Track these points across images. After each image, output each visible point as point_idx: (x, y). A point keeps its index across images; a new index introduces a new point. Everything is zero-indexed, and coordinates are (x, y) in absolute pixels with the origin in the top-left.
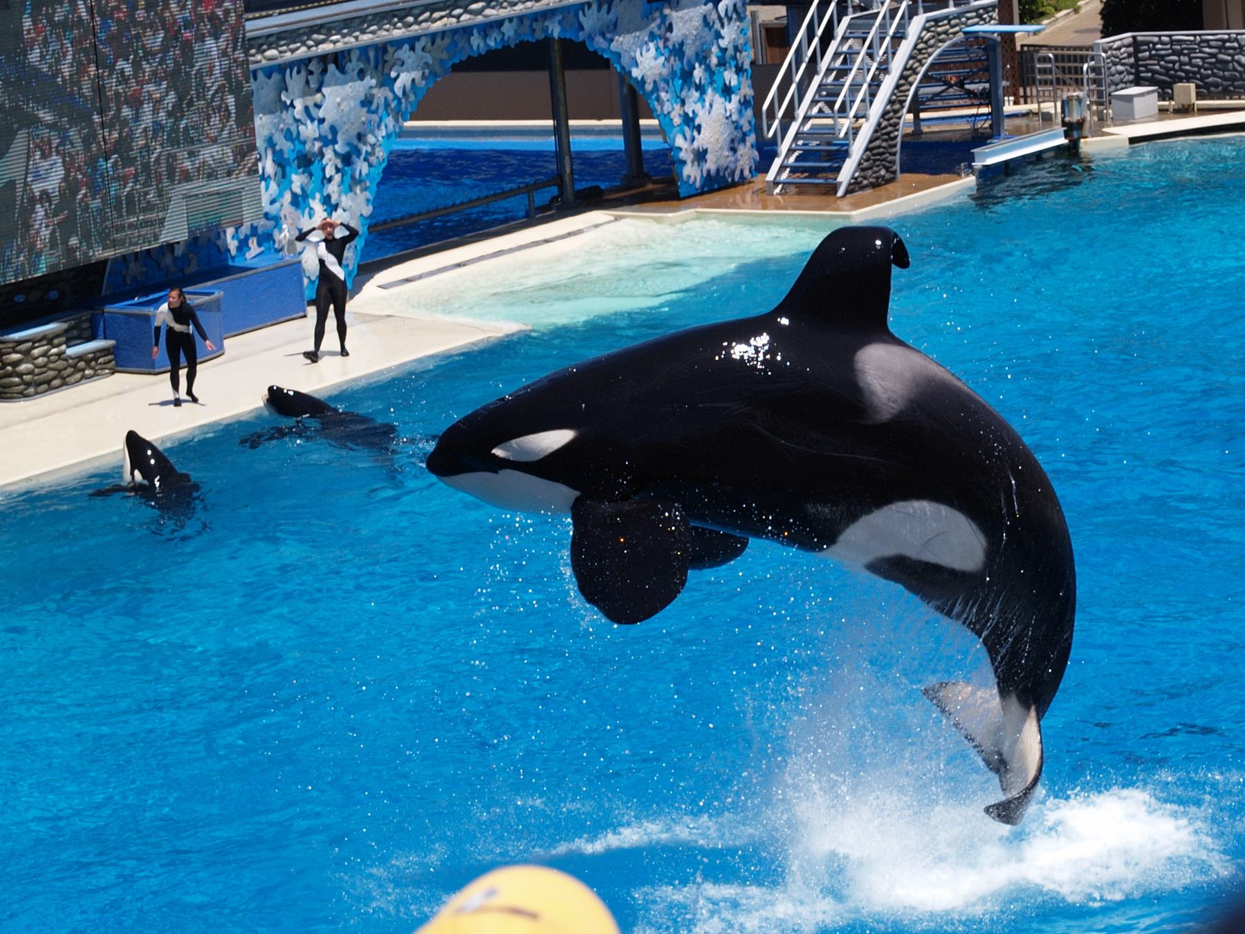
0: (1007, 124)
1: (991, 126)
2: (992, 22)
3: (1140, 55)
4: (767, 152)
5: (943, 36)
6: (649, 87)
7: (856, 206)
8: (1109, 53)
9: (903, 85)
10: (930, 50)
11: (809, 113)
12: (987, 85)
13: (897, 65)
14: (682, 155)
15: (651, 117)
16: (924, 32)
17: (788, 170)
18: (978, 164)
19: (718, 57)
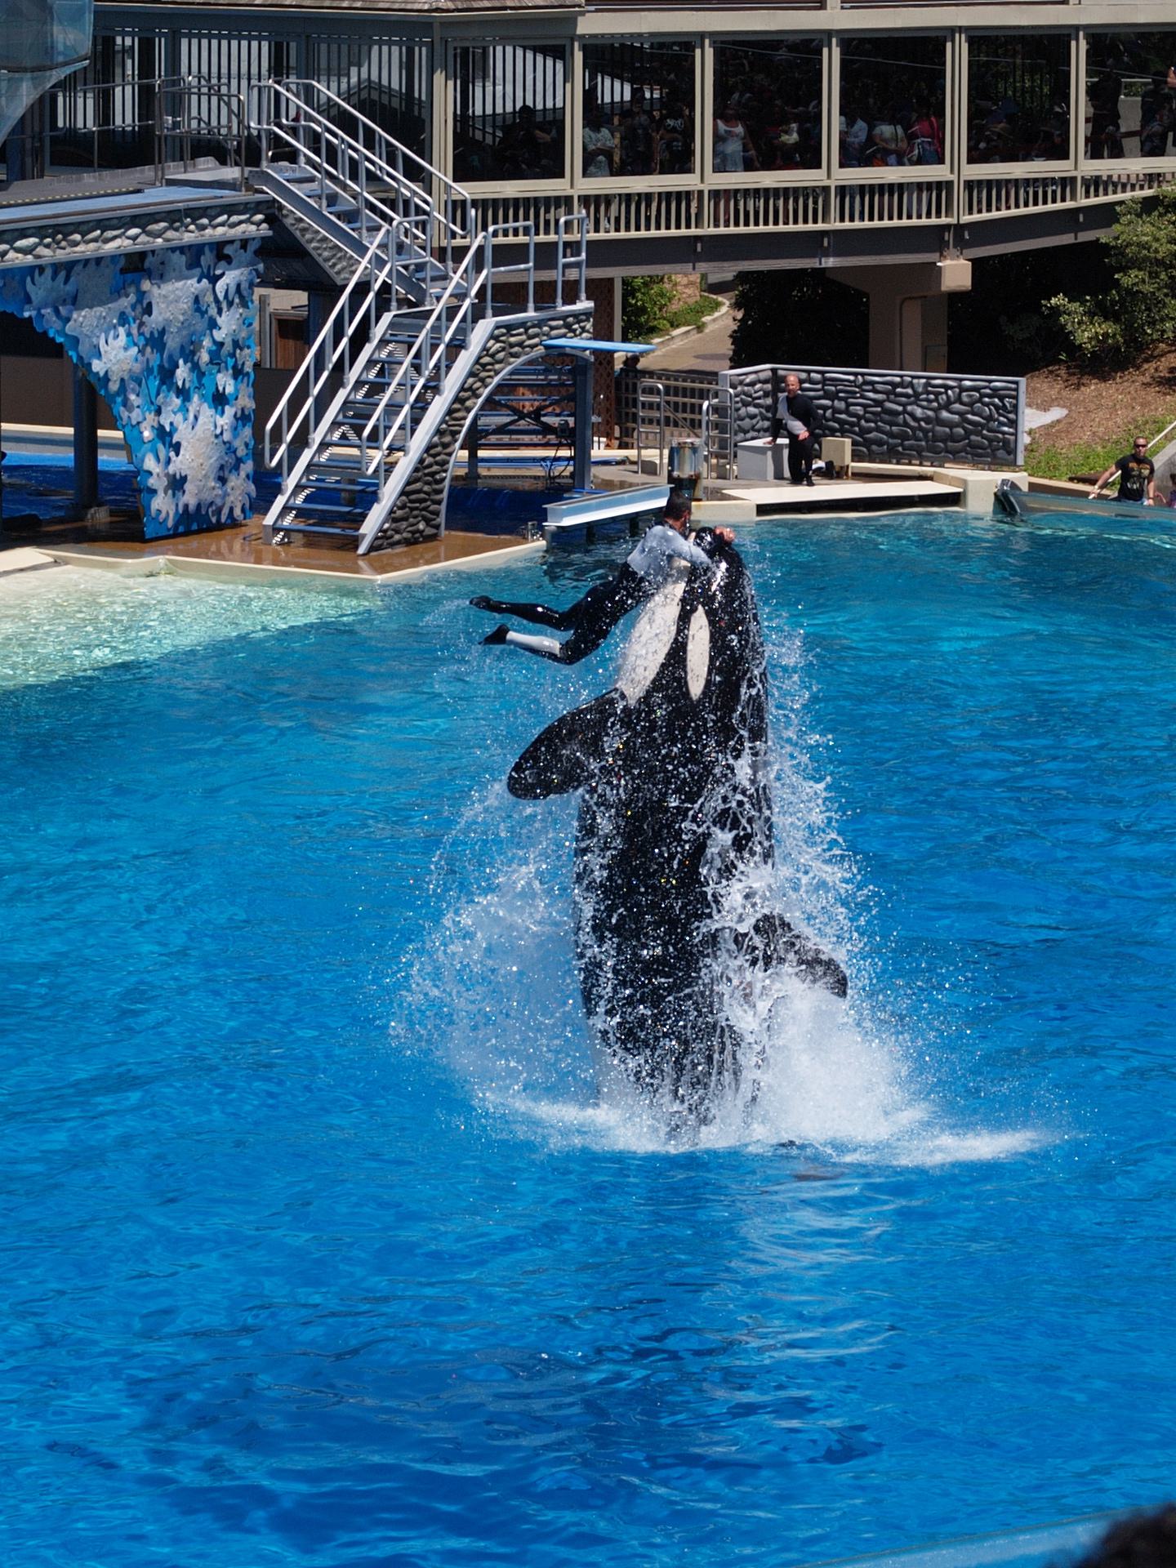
0: (595, 471)
1: (572, 475)
2: (584, 335)
4: (267, 485)
5: (516, 349)
6: (114, 387)
7: (382, 570)
8: (739, 389)
9: (458, 410)
10: (497, 366)
11: (328, 439)
12: (571, 421)
13: (452, 383)
14: (152, 482)
15: (116, 428)
16: (492, 342)
18: (551, 524)
19: (210, 352)
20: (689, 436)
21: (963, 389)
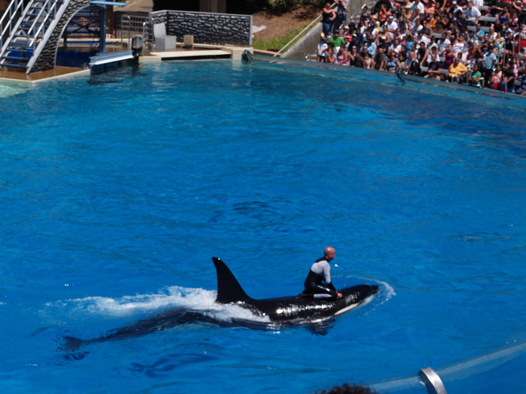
0: (107, 46)
1: (99, 47)
3: (170, 21)
5: (80, 4)
10: (74, 10)
11: (16, 34)
12: (99, 29)
17: (4, 60)
18: (92, 64)
20: (138, 34)
21: (231, 19)
